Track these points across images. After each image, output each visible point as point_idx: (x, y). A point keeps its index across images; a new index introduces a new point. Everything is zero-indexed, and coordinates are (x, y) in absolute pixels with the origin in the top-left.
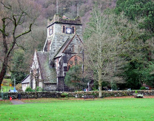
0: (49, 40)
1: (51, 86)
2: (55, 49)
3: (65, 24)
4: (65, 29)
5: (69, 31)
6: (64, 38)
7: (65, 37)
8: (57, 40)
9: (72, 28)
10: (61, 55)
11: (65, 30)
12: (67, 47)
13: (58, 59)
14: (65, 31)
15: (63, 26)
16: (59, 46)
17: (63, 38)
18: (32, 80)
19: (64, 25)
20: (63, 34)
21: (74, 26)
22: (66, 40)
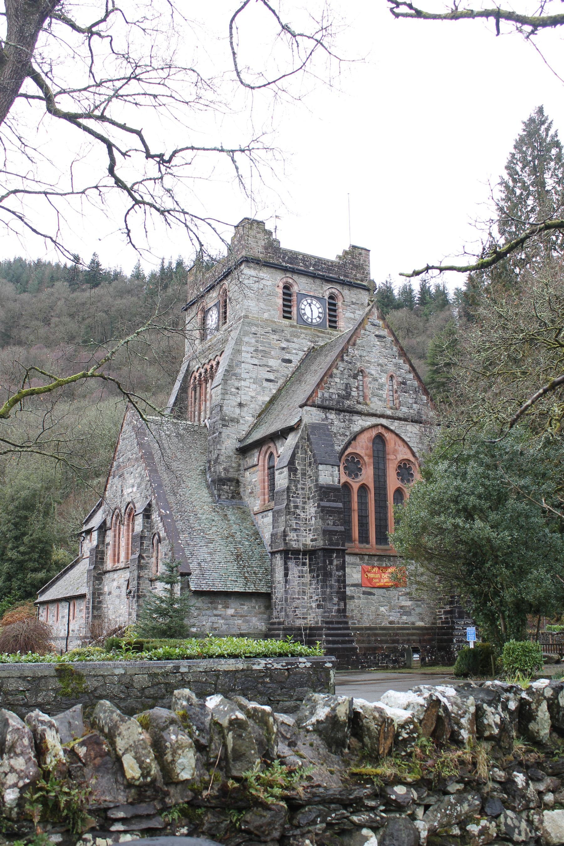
0: (195, 365)
1: (230, 611)
2: (244, 399)
3: (295, 277)
4: (294, 298)
5: (313, 311)
6: (293, 345)
7: (295, 340)
8: (253, 349)
9: (326, 298)
10: (296, 420)
11: (294, 303)
12: (329, 374)
13: (264, 449)
14: (294, 310)
15: (281, 285)
16: (266, 384)
17: (284, 346)
18: (98, 575)
19: (290, 281)
20: (287, 322)
21: (335, 289)
22: (301, 354)
